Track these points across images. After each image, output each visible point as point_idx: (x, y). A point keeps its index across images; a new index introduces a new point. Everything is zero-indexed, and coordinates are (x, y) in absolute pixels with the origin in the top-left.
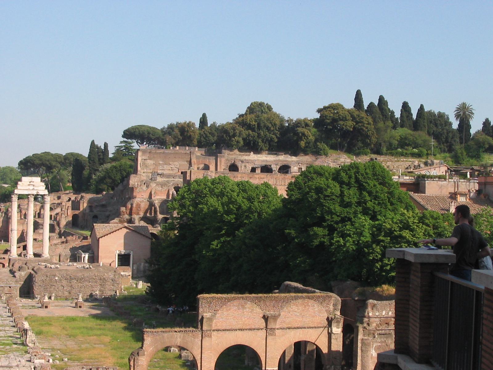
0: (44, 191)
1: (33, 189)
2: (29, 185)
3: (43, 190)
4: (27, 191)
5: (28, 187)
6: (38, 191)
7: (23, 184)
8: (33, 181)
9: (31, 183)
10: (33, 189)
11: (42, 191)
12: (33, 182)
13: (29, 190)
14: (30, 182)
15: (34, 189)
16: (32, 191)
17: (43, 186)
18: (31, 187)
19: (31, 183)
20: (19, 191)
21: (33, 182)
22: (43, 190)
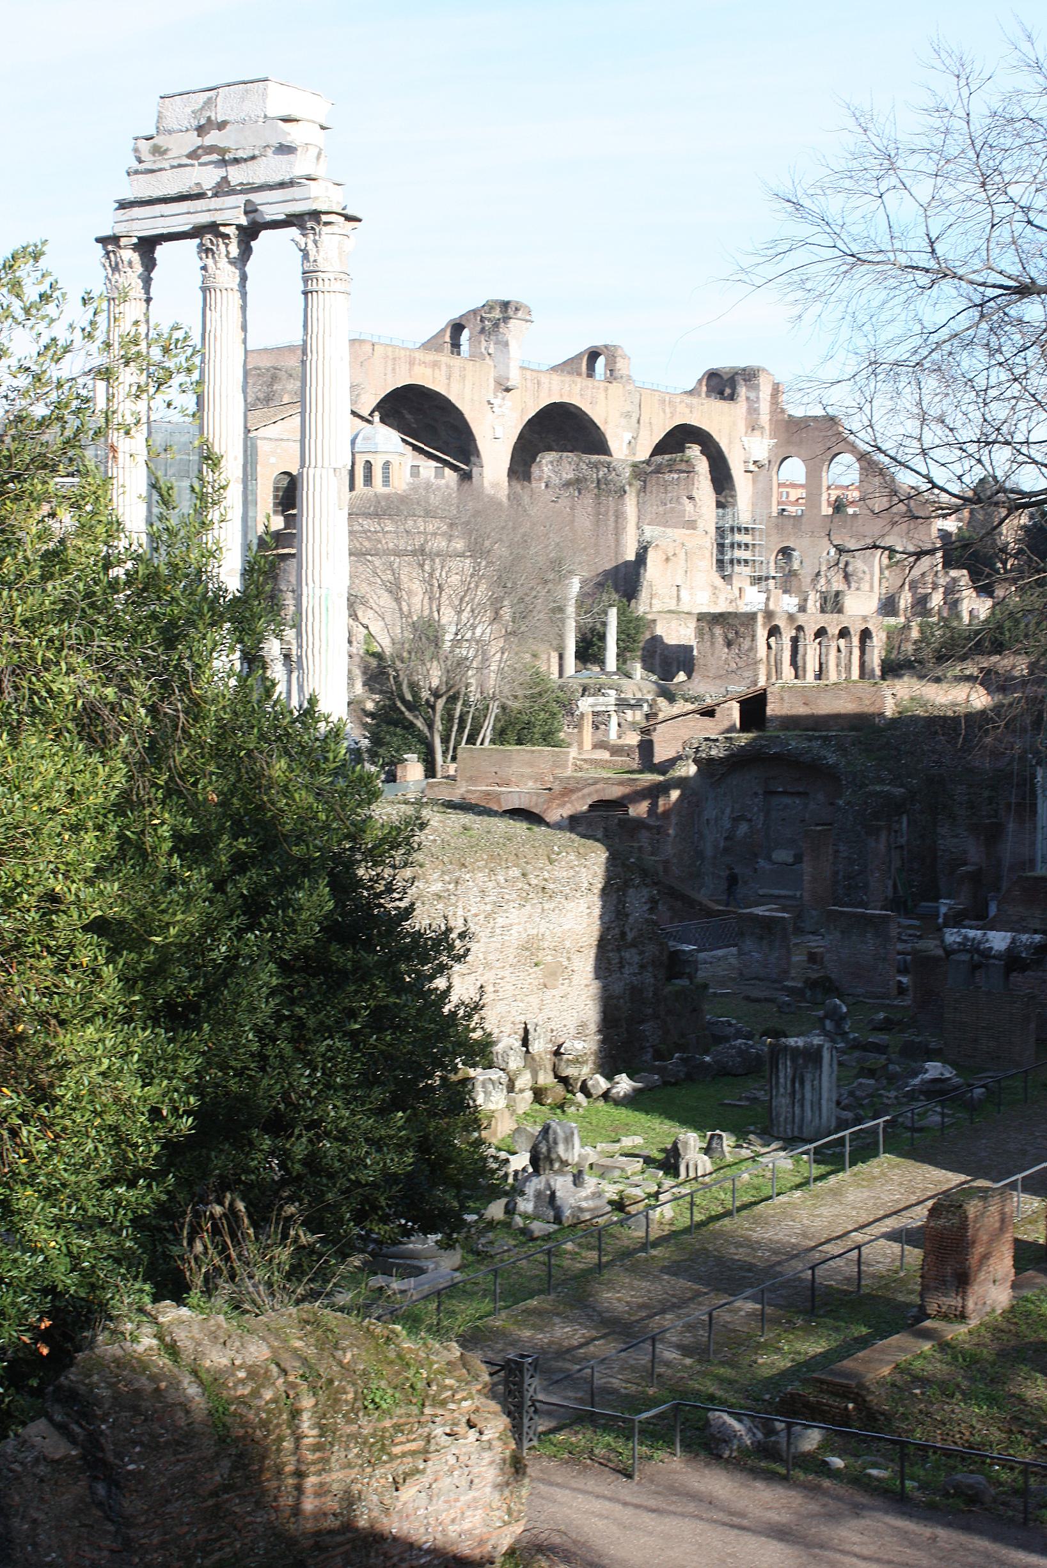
2: (193, 155)
9: (213, 138)
12: (222, 126)
15: (225, 179)
18: (208, 177)
19: (213, 138)
20: (137, 212)
21: (222, 126)
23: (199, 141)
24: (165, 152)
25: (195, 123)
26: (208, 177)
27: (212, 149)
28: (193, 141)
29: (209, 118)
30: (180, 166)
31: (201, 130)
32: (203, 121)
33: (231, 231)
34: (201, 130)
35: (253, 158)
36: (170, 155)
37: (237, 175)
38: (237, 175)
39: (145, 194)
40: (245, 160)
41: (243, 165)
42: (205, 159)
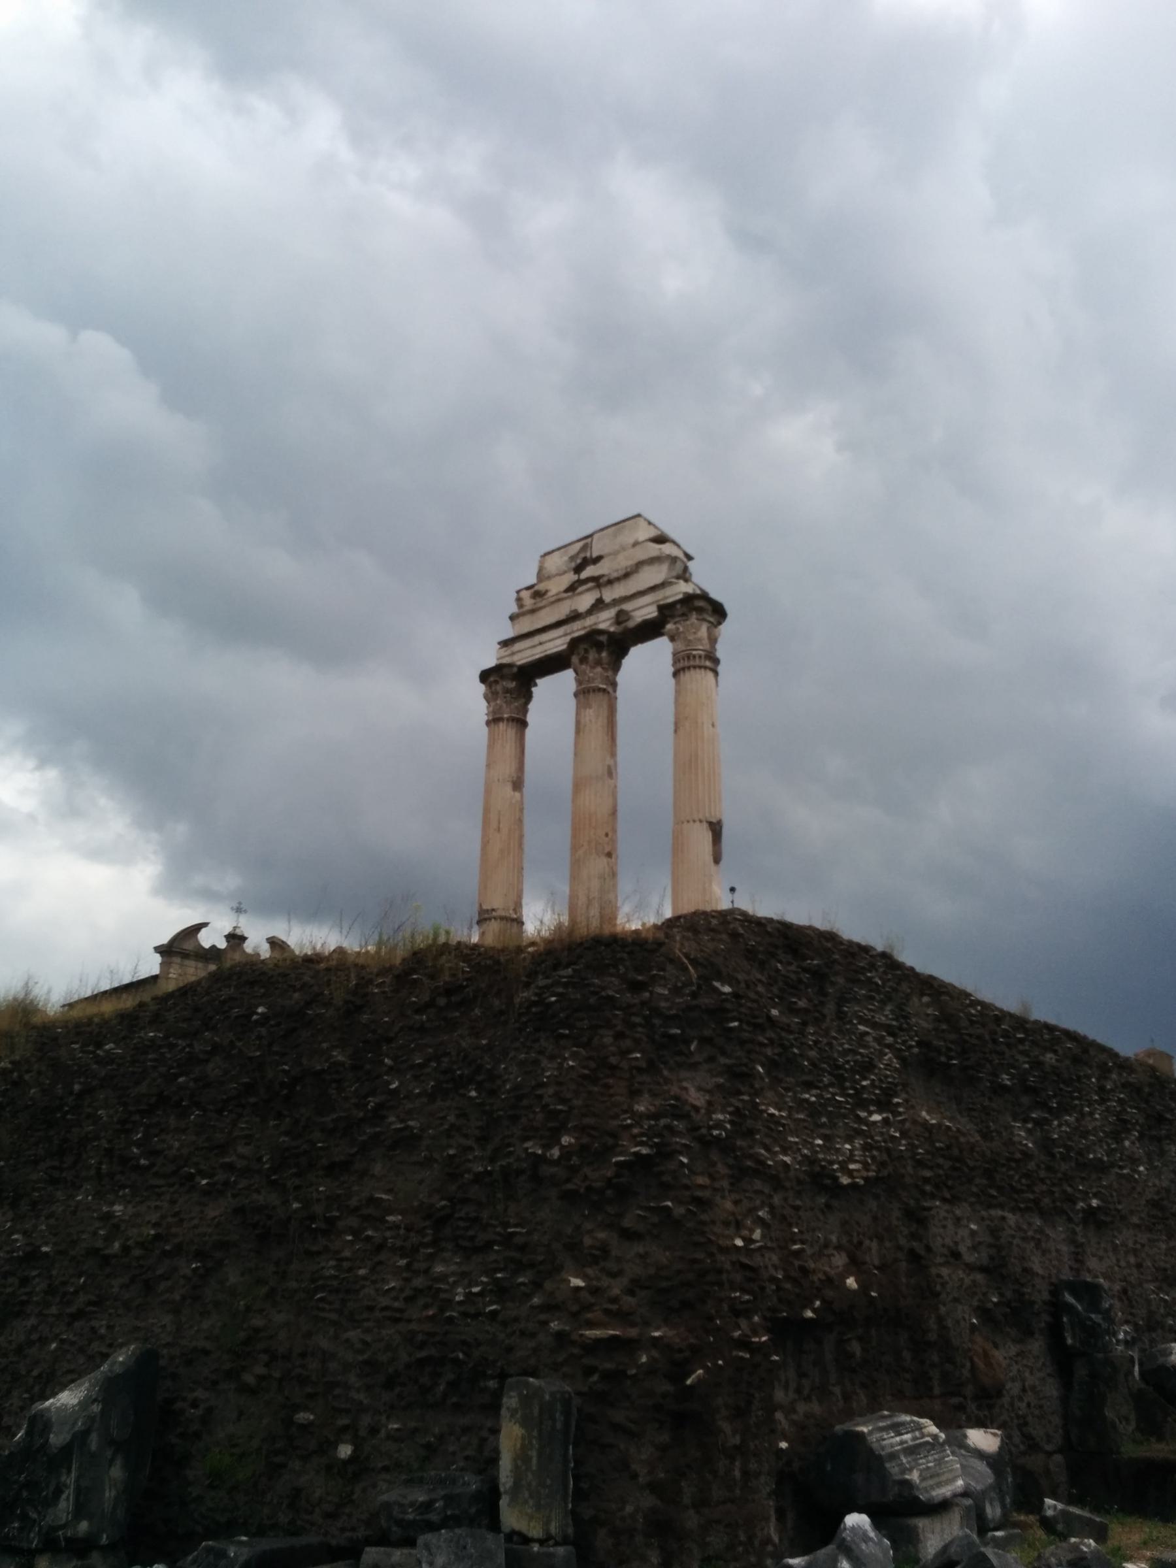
1: (599, 605)
2: (572, 588)
5: (562, 611)
8: (594, 555)
10: (599, 605)
13: (575, 617)
14: (578, 569)
16: (589, 622)
20: (518, 646)
21: (599, 559)
23: (576, 577)
24: (547, 591)
25: (573, 565)
26: (585, 601)
28: (571, 577)
30: (559, 600)
32: (579, 561)
33: (603, 638)
34: (578, 569)
35: (627, 575)
36: (550, 594)
37: (608, 595)
38: (608, 595)
39: (526, 630)
40: (618, 579)
42: (580, 589)
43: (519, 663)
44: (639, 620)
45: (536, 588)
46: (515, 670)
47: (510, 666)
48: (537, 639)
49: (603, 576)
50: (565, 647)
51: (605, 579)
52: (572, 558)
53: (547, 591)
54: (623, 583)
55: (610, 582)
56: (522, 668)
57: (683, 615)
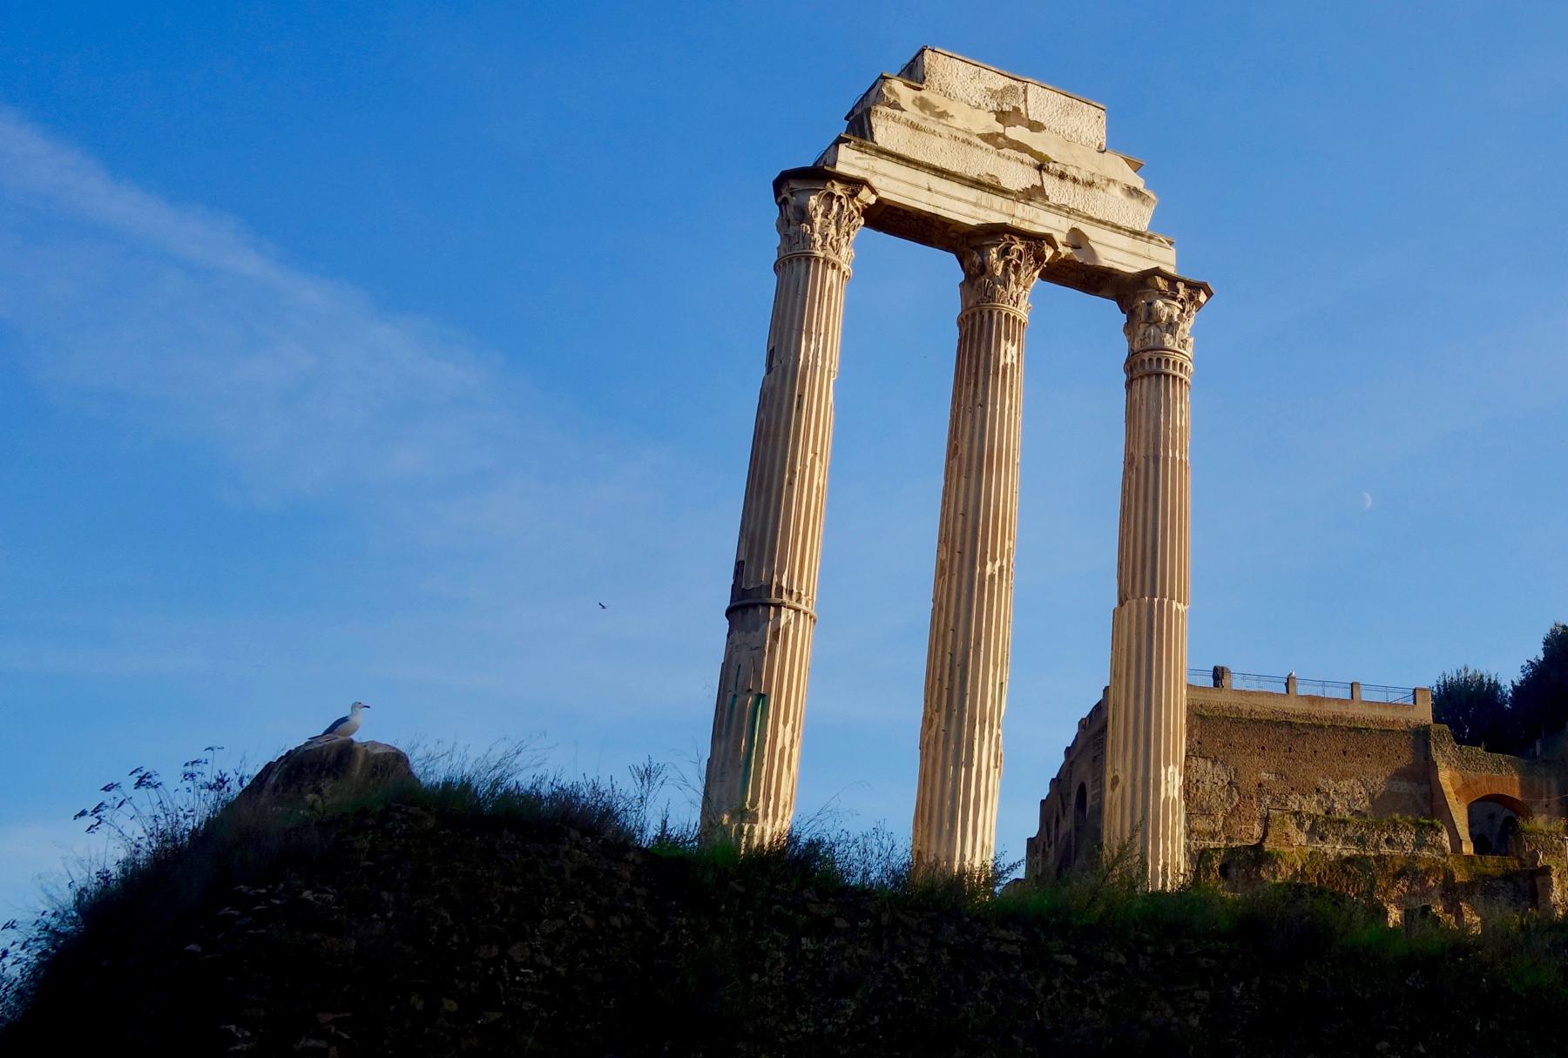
0: (1140, 246)
1: (1033, 194)
2: (990, 138)
3: (1135, 234)
4: (973, 194)
6: (1086, 228)
7: (924, 105)
9: (1017, 133)
10: (1033, 194)
11: (1124, 241)
12: (1036, 127)
17: (1132, 192)
18: (1017, 175)
19: (1017, 133)
20: (883, 165)
21: (1036, 127)
22: (1135, 234)
23: (999, 128)
25: (994, 105)
26: (1017, 175)
27: (1020, 147)
28: (986, 122)
29: (1017, 110)
31: (1001, 116)
32: (1006, 108)
33: (1049, 253)
35: (1090, 184)
36: (951, 122)
40: (1075, 180)
41: (1069, 183)
42: (1006, 151)
43: (882, 194)
44: (1105, 263)
45: (923, 94)
46: (872, 200)
47: (873, 191)
48: (924, 178)
49: (1048, 159)
50: (973, 222)
51: (1058, 168)
52: (993, 94)
53: (943, 114)
54: (1079, 189)
55: (1062, 176)
56: (880, 201)
57: (1182, 301)
